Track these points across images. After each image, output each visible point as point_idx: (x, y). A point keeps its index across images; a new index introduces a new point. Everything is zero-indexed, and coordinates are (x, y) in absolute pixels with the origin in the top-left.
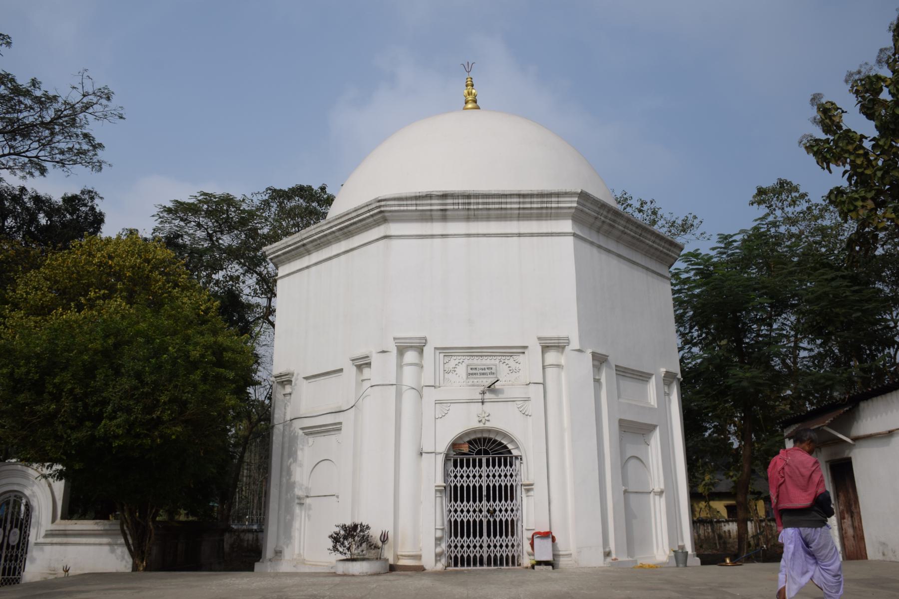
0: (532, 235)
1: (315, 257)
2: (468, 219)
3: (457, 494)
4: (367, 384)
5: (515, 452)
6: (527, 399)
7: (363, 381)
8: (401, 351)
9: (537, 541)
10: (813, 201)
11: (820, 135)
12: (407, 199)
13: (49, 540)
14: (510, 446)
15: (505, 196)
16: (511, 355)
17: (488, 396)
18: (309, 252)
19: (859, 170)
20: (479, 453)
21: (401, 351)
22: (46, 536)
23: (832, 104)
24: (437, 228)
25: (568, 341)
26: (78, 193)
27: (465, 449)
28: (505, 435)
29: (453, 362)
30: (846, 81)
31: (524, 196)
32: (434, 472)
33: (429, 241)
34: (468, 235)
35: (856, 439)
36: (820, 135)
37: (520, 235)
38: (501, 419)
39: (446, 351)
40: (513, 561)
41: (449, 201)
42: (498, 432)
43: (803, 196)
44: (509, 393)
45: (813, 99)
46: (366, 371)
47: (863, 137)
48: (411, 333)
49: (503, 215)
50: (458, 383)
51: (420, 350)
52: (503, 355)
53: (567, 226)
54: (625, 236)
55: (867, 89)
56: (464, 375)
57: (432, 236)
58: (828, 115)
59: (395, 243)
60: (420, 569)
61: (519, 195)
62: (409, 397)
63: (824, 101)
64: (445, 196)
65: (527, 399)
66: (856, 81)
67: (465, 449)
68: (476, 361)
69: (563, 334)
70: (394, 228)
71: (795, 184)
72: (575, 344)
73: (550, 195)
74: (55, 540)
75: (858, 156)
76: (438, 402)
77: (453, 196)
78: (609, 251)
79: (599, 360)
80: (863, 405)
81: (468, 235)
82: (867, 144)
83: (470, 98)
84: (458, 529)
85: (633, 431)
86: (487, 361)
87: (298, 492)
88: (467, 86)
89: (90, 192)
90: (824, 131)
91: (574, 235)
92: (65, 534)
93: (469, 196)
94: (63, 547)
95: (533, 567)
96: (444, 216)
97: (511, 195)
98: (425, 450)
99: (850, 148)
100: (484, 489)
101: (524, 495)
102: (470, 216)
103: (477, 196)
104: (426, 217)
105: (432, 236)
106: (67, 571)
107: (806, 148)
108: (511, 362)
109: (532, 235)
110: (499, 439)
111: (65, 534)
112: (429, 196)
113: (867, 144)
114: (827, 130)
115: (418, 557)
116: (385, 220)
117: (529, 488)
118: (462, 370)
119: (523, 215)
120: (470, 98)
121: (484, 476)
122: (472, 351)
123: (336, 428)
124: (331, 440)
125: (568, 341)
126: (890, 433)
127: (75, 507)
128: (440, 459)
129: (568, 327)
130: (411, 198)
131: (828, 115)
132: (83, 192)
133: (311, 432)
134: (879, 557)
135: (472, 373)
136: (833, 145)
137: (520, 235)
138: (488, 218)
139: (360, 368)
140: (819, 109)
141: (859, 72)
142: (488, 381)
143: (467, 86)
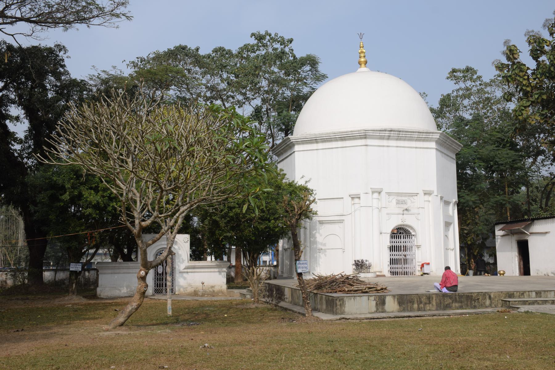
0: (421, 148)
1: (321, 146)
2: (397, 139)
3: (392, 249)
4: (357, 206)
5: (413, 233)
6: (419, 214)
7: (354, 204)
8: (373, 192)
9: (425, 266)
10: (484, 81)
11: (505, 62)
12: (376, 131)
13: (186, 270)
14: (411, 231)
15: (414, 132)
16: (412, 196)
17: (405, 212)
18: (317, 142)
19: (524, 88)
20: (400, 233)
21: (373, 192)
22: (185, 269)
23: (515, 47)
24: (385, 142)
25: (433, 192)
26: (53, 46)
27: (395, 232)
28: (412, 228)
29: (391, 198)
30: (525, 35)
31: (420, 133)
32: (387, 241)
33: (382, 148)
34: (397, 147)
35: (531, 233)
36: (505, 62)
37: (416, 148)
38: (408, 221)
39: (389, 194)
40: (412, 274)
41: (392, 133)
42: (407, 226)
43: (479, 78)
44: (413, 211)
45: (505, 42)
46: (356, 200)
47: (528, 68)
48: (377, 186)
49: (411, 139)
50: (393, 205)
51: (380, 193)
52: (409, 196)
53: (433, 145)
54: (445, 145)
55: (537, 47)
56: (395, 203)
57: (384, 146)
58: (511, 53)
59: (369, 148)
60: (384, 276)
61: (419, 132)
62: (376, 211)
63: (511, 44)
64: (391, 131)
65: (419, 214)
66: (531, 36)
67: (395, 232)
68: (400, 198)
69: (432, 189)
70: (369, 142)
71: (475, 69)
72: (435, 193)
73: (430, 133)
74: (189, 270)
75: (524, 79)
76: (388, 214)
77: (394, 131)
78: (448, 156)
79: (442, 198)
80: (535, 221)
81: (397, 147)
82: (529, 72)
83: (362, 55)
84: (393, 262)
85: (448, 225)
86: (404, 198)
87: (320, 246)
88: (360, 47)
89: (59, 45)
90: (507, 59)
91: (436, 149)
92: (194, 267)
93: (400, 131)
94: (192, 274)
95: (422, 275)
96: (389, 138)
97: (416, 132)
98: (383, 232)
99: (521, 74)
100: (402, 247)
101: (416, 249)
102: (398, 139)
103: (403, 132)
104: (382, 138)
105: (384, 146)
106: (203, 284)
107: (496, 67)
108: (412, 198)
109: (421, 148)
110: (407, 228)
111: (194, 267)
112: (385, 130)
113: (529, 72)
114: (508, 59)
115: (381, 272)
116: (365, 138)
117: (418, 247)
118: (394, 202)
119: (418, 140)
120: (362, 55)
121: (401, 242)
122: (398, 194)
123: (341, 221)
124: (336, 227)
125: (433, 192)
126: (546, 233)
127: (197, 254)
128: (389, 235)
129: (433, 186)
130: (378, 131)
131: (511, 53)
132: (56, 46)
133: (321, 222)
134: (536, 274)
135: (398, 202)
136: (511, 69)
137: (416, 148)
138: (405, 140)
139: (353, 198)
140: (507, 48)
141: (533, 31)
142: (405, 207)
143: (360, 47)
